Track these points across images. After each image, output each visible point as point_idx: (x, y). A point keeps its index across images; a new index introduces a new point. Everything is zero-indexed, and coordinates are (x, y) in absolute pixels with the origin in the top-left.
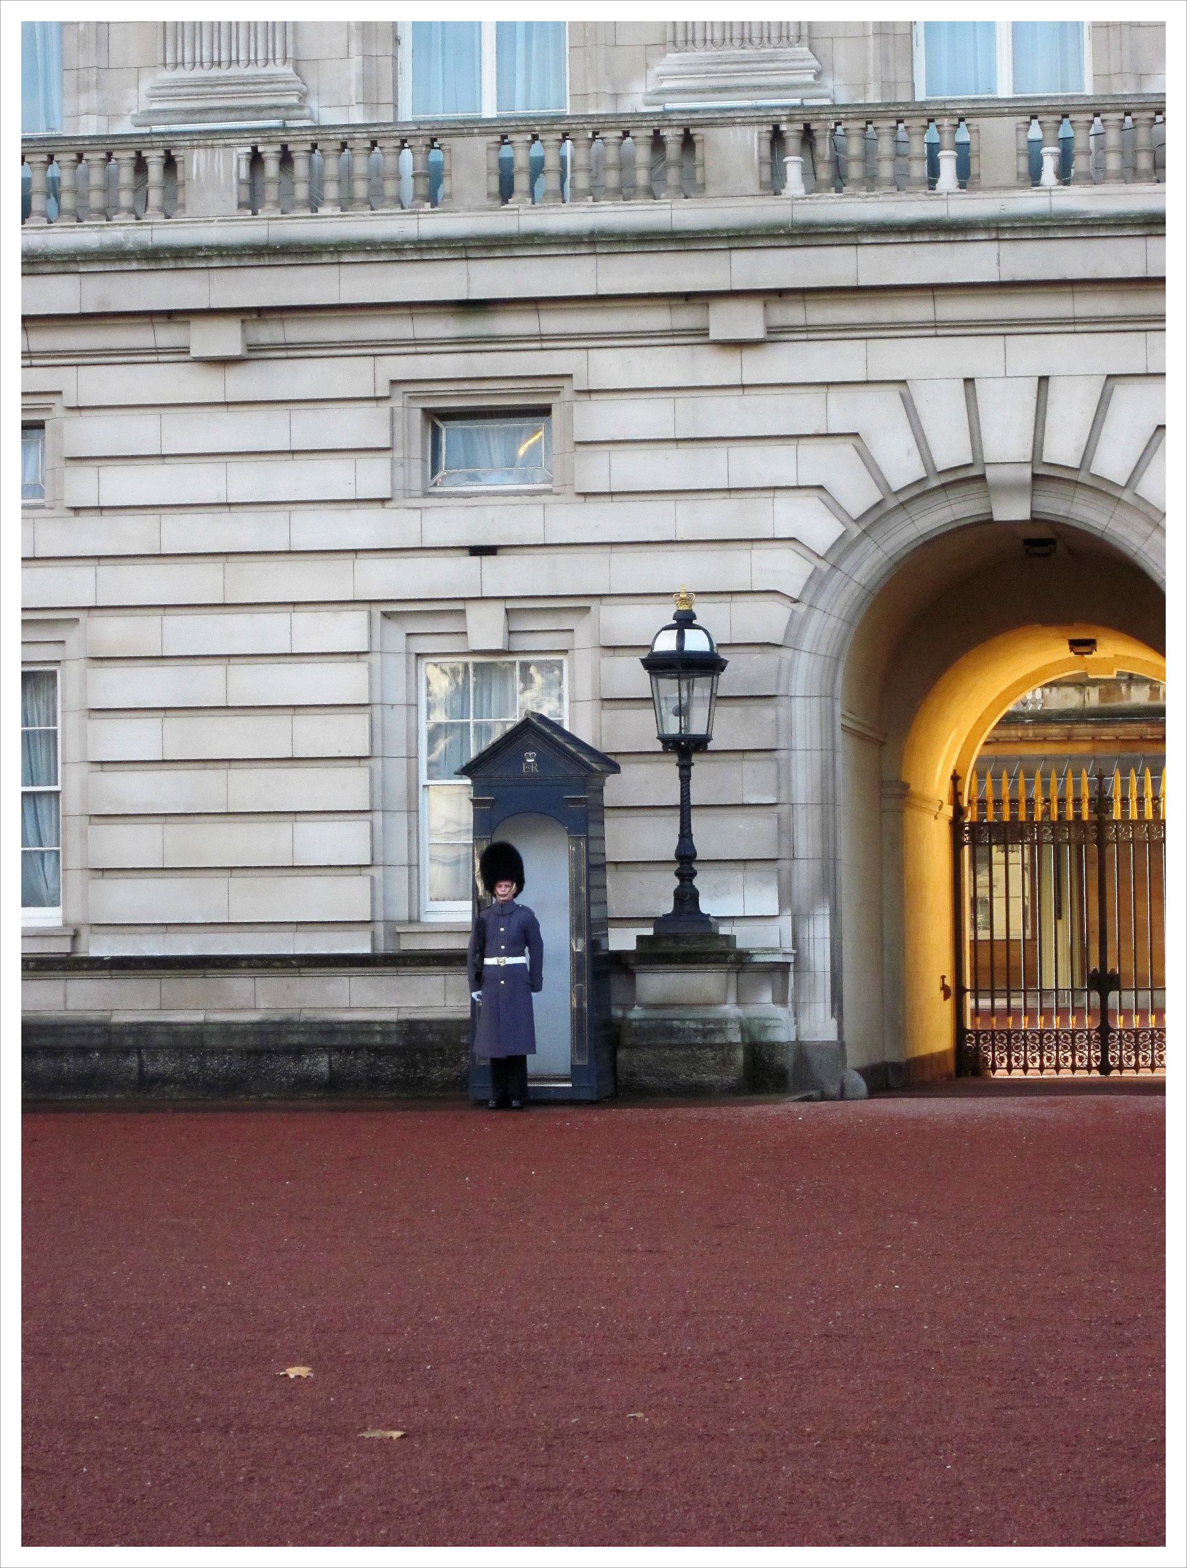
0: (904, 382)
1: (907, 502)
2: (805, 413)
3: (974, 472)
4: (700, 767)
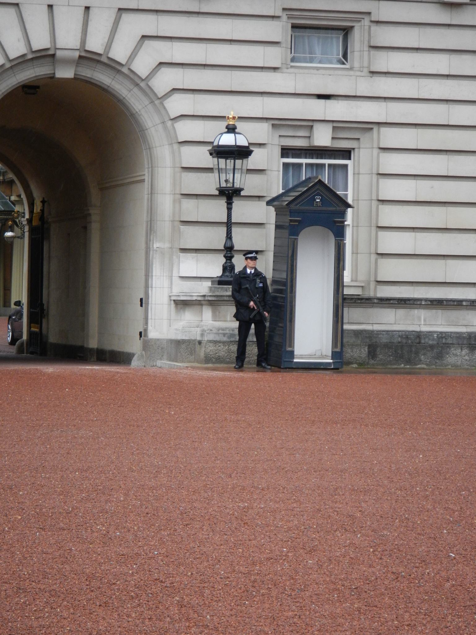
0: (17, 5)
1: (15, 65)
3: (51, 52)
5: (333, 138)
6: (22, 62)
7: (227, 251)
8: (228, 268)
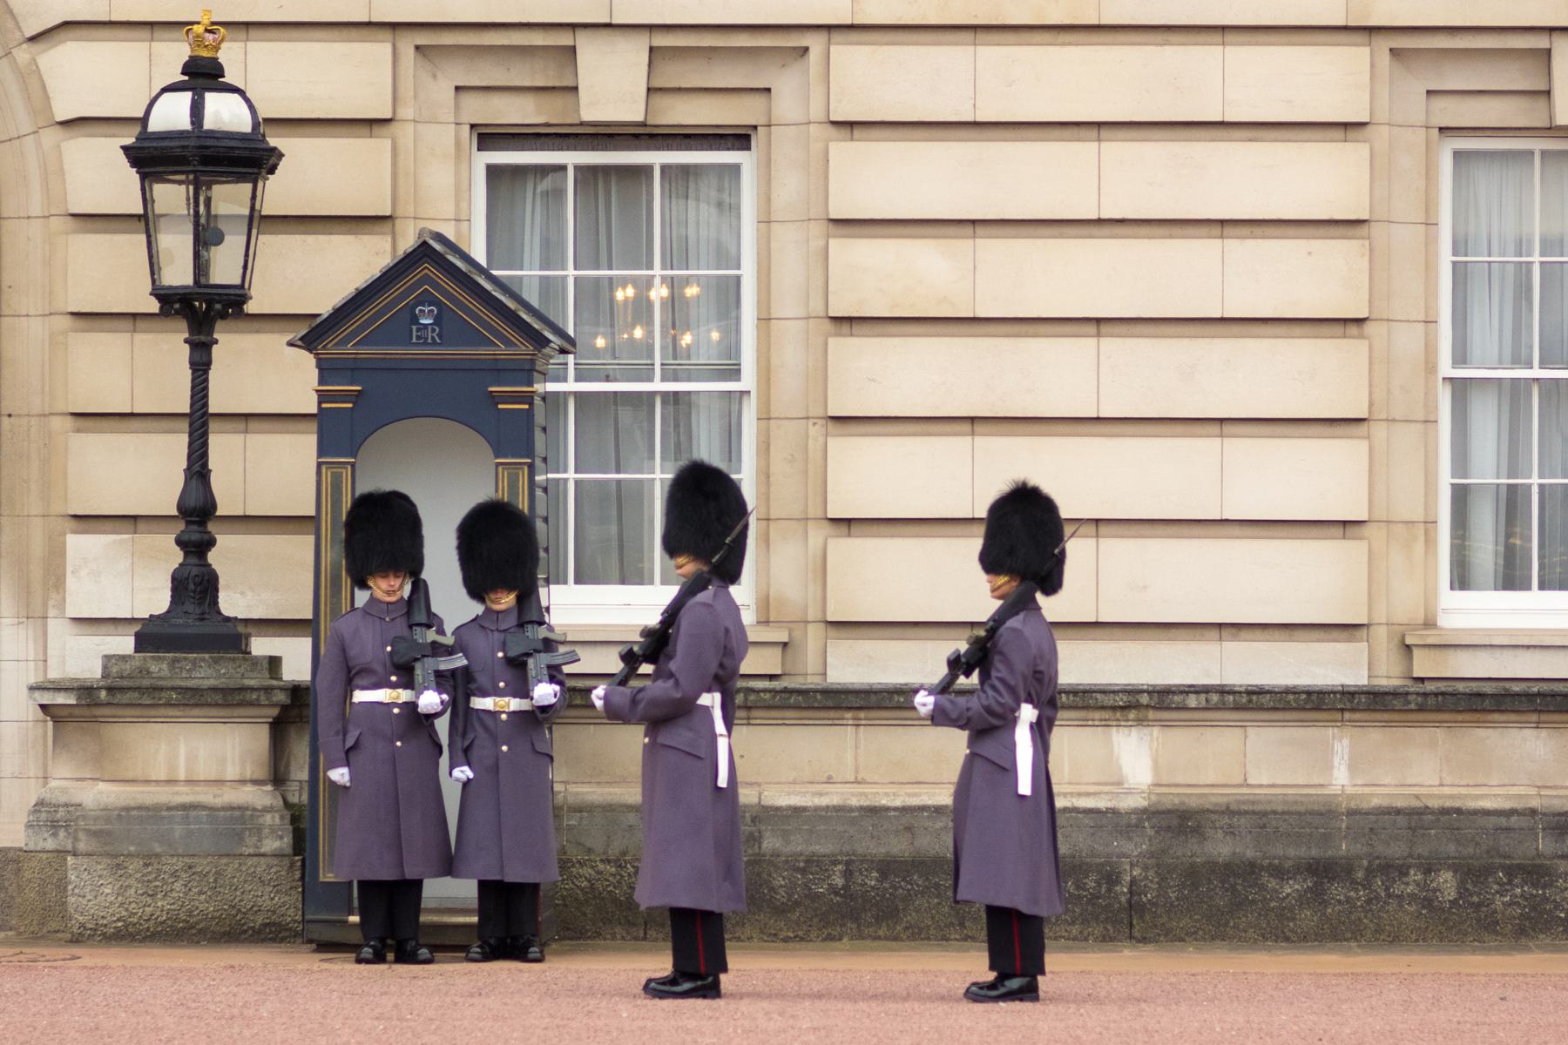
5: (650, 90)
7: (188, 523)
8: (196, 585)
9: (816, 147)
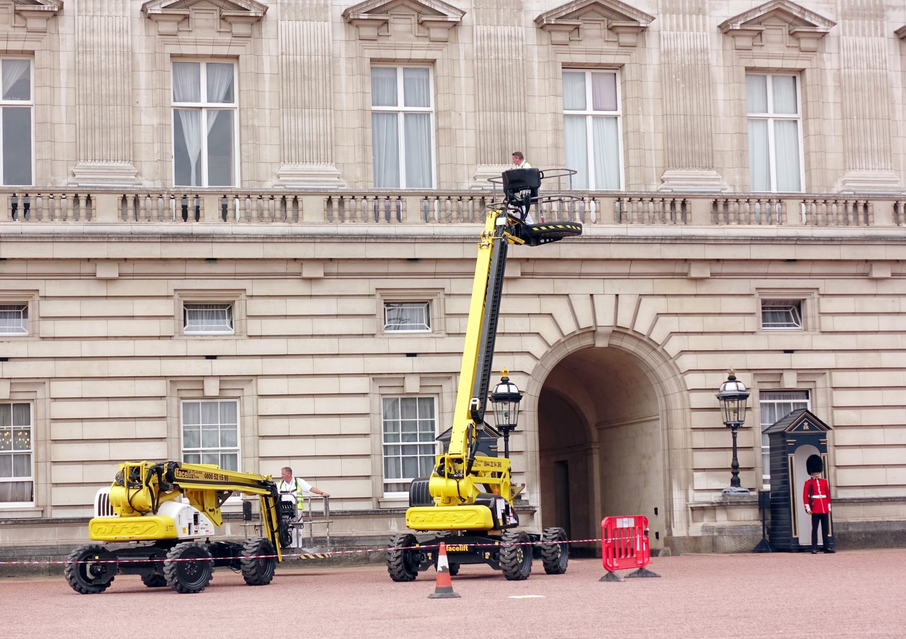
2: (533, 305)
3: (594, 329)
4: (512, 437)
6: (573, 336)
9: (829, 393)
